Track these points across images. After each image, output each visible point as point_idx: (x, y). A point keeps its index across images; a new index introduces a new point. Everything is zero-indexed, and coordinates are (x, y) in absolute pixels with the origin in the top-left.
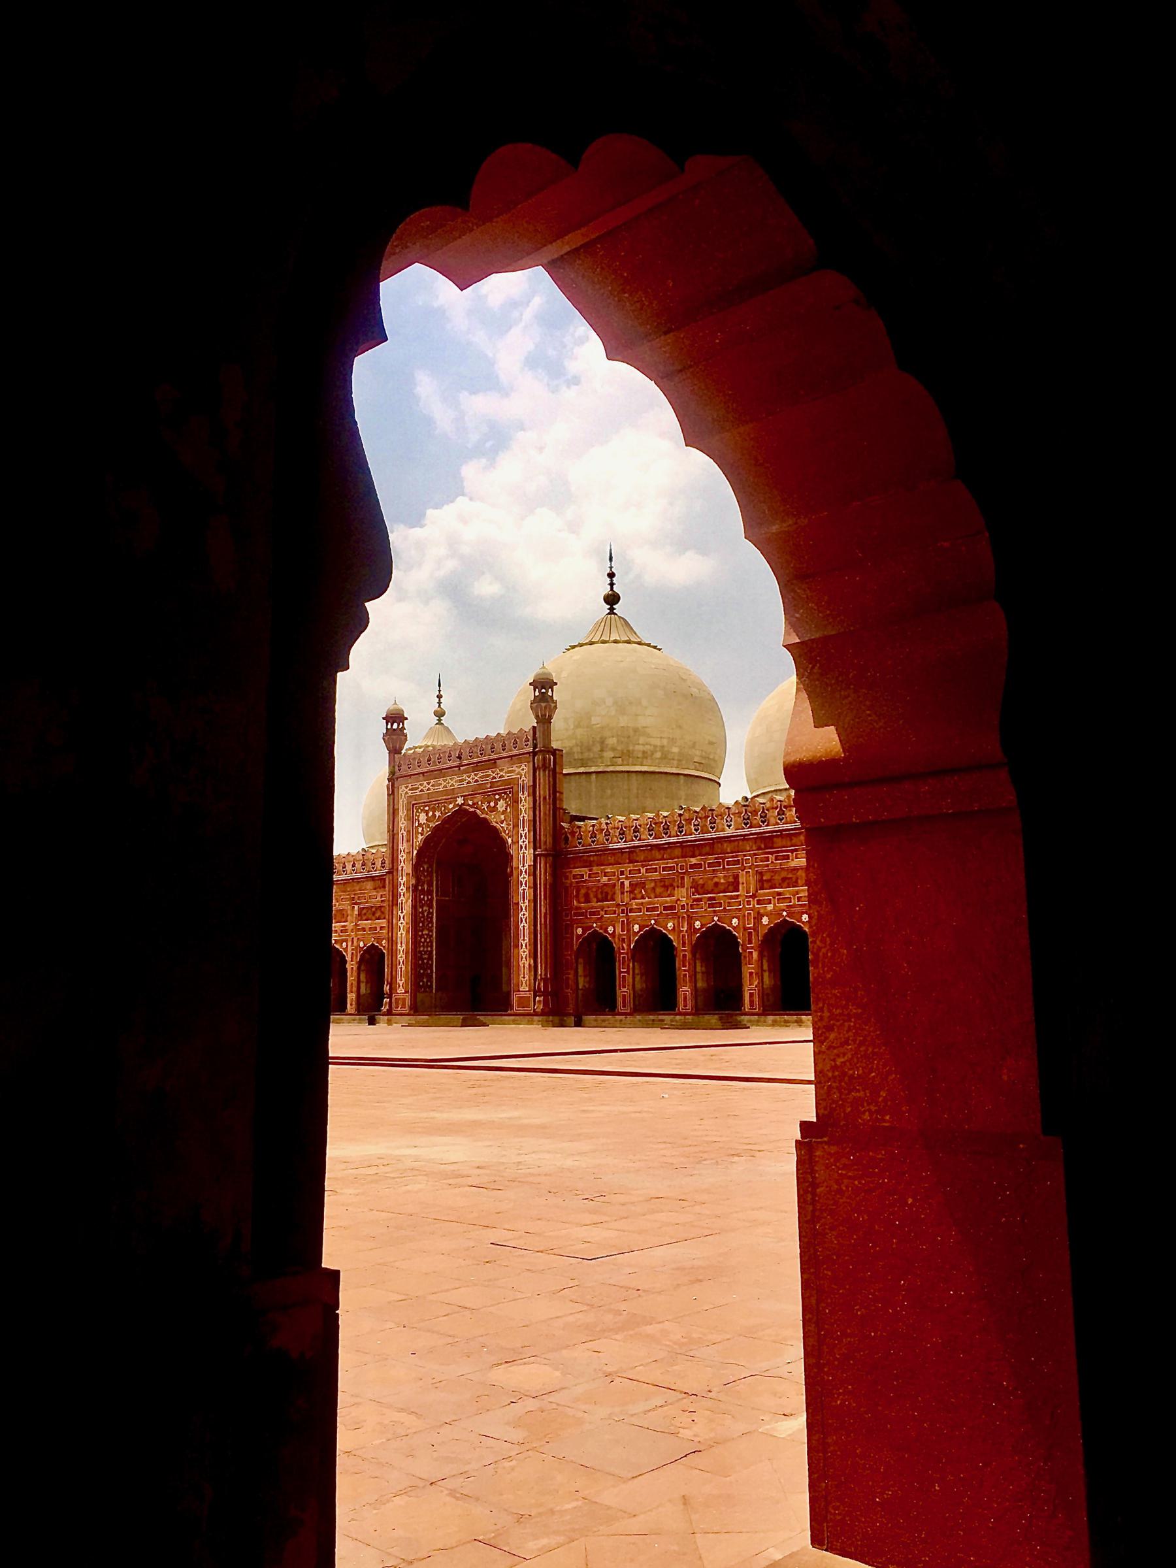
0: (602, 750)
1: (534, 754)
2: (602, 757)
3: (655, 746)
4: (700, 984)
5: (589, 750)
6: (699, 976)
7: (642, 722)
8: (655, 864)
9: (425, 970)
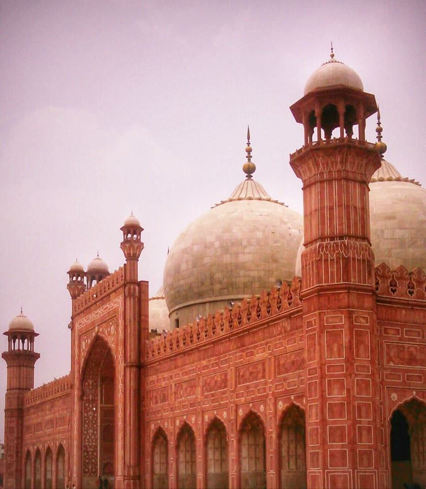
0: (212, 284)
1: (125, 285)
2: (212, 290)
3: (254, 278)
4: (212, 470)
5: (203, 284)
6: (211, 463)
7: (242, 258)
8: (188, 368)
9: (90, 460)
